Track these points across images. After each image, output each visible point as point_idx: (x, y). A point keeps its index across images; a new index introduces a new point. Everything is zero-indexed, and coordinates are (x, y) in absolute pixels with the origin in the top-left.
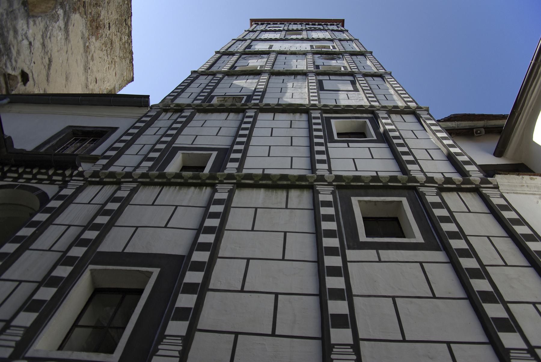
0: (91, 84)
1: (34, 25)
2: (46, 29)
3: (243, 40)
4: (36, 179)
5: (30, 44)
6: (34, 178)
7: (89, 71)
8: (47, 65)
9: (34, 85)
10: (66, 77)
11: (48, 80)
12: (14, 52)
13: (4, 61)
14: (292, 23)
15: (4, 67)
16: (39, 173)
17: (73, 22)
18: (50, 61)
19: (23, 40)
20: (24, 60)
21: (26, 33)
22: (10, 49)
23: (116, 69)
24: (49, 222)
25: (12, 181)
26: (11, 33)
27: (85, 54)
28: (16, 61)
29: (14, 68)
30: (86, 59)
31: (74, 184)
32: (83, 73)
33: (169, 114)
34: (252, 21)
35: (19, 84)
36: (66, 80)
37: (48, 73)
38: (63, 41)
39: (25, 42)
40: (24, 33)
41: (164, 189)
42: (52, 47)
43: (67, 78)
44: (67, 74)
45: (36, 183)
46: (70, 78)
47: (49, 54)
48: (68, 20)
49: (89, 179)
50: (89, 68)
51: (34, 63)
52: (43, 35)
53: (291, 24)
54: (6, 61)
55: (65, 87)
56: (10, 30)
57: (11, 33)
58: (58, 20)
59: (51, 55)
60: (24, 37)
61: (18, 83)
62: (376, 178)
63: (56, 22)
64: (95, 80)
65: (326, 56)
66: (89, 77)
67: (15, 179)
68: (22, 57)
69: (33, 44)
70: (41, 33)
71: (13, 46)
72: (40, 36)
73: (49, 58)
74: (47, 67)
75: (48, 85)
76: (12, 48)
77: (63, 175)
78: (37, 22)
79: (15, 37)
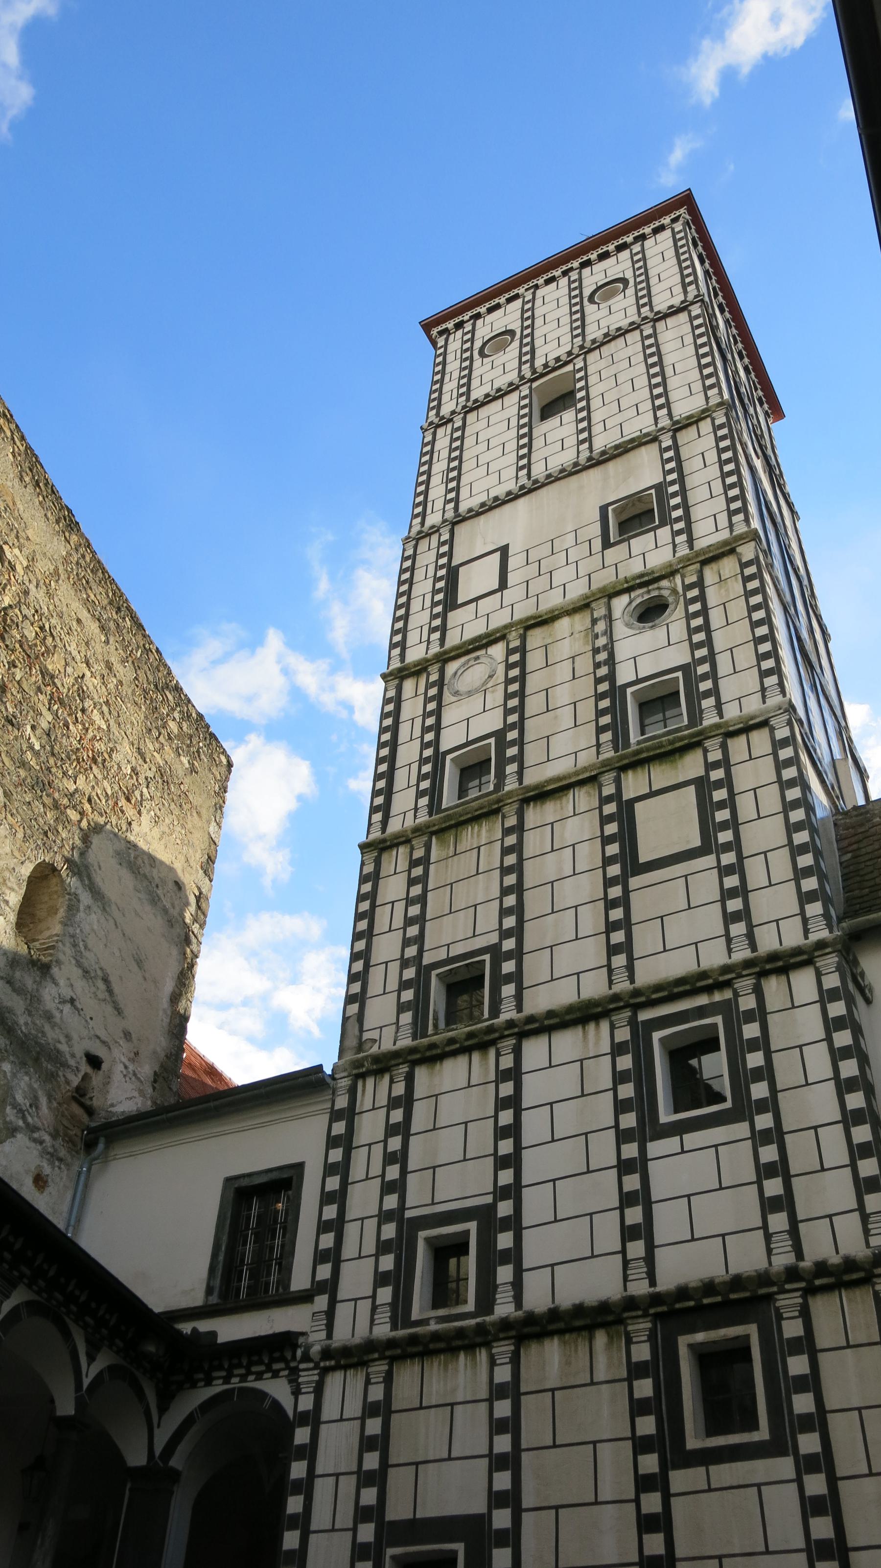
0: (174, 908)
1: (60, 969)
2: (75, 945)
3: (429, 535)
4: (252, 1373)
5: (72, 1001)
6: (249, 1373)
7: (160, 892)
8: (107, 994)
9: (110, 1048)
10: (138, 963)
11: (119, 1011)
12: (63, 1047)
13: (63, 1079)
14: (541, 281)
15: (68, 1088)
16: (251, 1364)
17: (96, 864)
18: (106, 980)
19: (62, 1011)
20: (79, 1036)
21: (59, 995)
22: (58, 1051)
23: (195, 803)
24: (311, 1473)
25: (224, 1383)
26: (47, 1028)
27: (139, 877)
28: (73, 1056)
29: (77, 1068)
30: (145, 883)
31: (308, 1377)
32: (154, 914)
33: (370, 1082)
34: (427, 326)
35: (94, 1078)
36: (141, 969)
37: (114, 1002)
38: (103, 920)
39: (67, 1008)
40: (57, 1001)
41: (425, 1365)
42: (96, 955)
43: (139, 963)
44: (136, 956)
45: (256, 1380)
46: (143, 954)
47: (99, 973)
48: (89, 877)
49: (322, 1364)
50: (157, 886)
51: (91, 1019)
52: (77, 961)
53: (537, 287)
54: (64, 1076)
55: (145, 979)
56: (43, 1026)
57: (47, 1028)
58: (79, 901)
59: (101, 969)
60: (61, 1007)
61: (91, 1078)
62: (709, 1287)
63: (78, 910)
64: (175, 888)
65: (642, 595)
66: (165, 903)
67: (227, 1380)
68: (75, 1036)
69: (75, 997)
70: (74, 962)
71: (60, 1042)
72: (75, 969)
73: (103, 979)
74: (106, 995)
75: (123, 1018)
76: (59, 1046)
77: (282, 1359)
78: (61, 957)
79: (54, 1026)
